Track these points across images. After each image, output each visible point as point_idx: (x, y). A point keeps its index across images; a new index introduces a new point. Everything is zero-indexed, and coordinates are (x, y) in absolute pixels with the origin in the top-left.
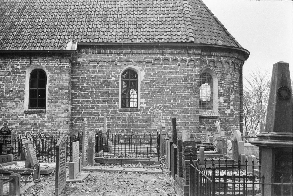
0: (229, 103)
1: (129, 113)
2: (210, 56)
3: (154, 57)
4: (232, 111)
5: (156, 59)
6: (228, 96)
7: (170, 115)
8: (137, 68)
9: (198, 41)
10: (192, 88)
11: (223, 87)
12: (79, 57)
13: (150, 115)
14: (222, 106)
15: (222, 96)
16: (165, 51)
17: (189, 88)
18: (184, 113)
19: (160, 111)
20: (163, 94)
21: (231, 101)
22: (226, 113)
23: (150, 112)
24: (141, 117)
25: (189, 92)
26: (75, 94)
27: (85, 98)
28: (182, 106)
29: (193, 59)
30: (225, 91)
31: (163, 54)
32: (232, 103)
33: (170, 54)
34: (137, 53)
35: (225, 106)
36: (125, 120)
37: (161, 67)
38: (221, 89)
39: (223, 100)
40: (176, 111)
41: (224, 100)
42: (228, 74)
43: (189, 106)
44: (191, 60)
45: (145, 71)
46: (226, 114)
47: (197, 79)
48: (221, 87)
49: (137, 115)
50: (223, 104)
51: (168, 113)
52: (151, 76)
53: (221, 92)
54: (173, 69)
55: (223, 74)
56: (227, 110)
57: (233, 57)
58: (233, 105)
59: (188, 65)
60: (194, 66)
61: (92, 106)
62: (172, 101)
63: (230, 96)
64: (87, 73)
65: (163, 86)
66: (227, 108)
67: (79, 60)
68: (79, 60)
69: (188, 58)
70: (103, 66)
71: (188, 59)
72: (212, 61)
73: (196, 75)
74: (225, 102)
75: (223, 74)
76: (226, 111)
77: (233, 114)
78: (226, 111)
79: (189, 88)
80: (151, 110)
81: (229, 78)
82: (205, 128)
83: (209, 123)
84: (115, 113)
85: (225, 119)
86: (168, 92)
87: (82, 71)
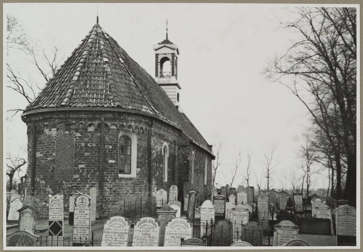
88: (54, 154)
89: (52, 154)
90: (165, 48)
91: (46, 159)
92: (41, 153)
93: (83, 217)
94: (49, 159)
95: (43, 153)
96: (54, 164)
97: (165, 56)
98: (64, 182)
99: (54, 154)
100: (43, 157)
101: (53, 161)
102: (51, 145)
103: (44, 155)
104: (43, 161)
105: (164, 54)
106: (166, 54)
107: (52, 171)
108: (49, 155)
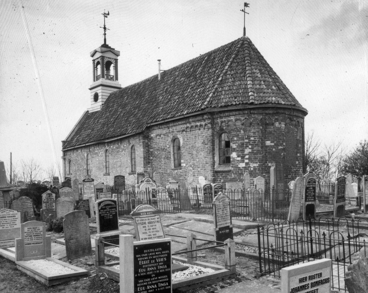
0: (243, 157)
2: (221, 117)
3: (186, 126)
4: (247, 164)
5: (187, 128)
6: (242, 150)
9: (235, 102)
11: (236, 143)
12: (152, 134)
14: (235, 161)
15: (236, 152)
16: (191, 120)
22: (239, 166)
26: (153, 159)
27: (157, 162)
30: (238, 147)
31: (190, 123)
32: (247, 157)
33: (193, 122)
34: (176, 125)
35: (238, 161)
38: (234, 145)
41: (237, 155)
44: (206, 125)
45: (183, 138)
46: (240, 168)
47: (210, 140)
48: (233, 144)
50: (236, 159)
52: (186, 141)
53: (234, 149)
56: (241, 164)
57: (244, 114)
58: (249, 159)
59: (204, 129)
60: (209, 129)
61: (160, 167)
63: (244, 151)
64: (156, 144)
66: (241, 162)
67: (152, 135)
68: (152, 135)
69: (203, 123)
70: (162, 138)
71: (204, 124)
72: (224, 122)
74: (238, 156)
76: (239, 165)
78: (239, 165)
80: (187, 168)
82: (220, 181)
83: (224, 177)
85: (239, 172)
87: (154, 143)
88: (284, 144)
89: (283, 144)
91: (278, 148)
92: (271, 142)
93: (152, 230)
94: (280, 147)
96: (285, 152)
98: (292, 167)
99: (284, 144)
100: (273, 146)
101: (284, 149)
102: (280, 136)
103: (275, 144)
104: (274, 149)
105: (109, 58)
106: (110, 58)
107: (284, 158)
108: (280, 144)
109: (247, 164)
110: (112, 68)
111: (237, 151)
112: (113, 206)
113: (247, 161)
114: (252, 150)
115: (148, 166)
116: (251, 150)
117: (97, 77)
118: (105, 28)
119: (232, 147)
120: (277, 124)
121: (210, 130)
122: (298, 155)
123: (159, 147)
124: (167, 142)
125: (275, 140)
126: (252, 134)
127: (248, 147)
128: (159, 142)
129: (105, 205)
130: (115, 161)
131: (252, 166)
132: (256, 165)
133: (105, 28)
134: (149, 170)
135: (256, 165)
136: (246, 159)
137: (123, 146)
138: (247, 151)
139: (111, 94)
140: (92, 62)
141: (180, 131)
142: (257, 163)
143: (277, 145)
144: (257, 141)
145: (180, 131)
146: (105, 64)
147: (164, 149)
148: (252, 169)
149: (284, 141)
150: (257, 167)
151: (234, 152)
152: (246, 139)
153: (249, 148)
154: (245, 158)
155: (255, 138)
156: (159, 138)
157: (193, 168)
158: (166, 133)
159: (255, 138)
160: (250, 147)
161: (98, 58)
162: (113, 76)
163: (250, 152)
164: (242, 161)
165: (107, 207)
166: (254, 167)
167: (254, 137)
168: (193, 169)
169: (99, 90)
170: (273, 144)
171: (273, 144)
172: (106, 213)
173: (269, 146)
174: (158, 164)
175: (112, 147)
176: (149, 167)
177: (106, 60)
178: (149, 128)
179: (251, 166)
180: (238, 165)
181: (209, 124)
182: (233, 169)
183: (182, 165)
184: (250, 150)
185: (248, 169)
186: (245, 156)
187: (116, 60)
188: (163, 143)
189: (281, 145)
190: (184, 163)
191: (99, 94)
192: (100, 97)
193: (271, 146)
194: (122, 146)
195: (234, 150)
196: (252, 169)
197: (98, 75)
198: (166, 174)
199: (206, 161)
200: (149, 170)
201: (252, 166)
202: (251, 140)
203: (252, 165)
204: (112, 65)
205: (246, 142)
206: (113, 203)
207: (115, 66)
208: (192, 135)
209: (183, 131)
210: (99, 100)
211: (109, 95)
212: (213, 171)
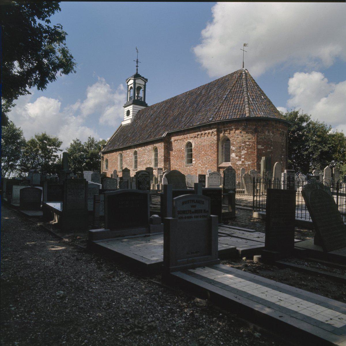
0: (240, 157)
1: (188, 167)
4: (243, 162)
5: (198, 135)
6: (239, 152)
7: (204, 167)
8: (191, 141)
10: (213, 149)
13: (197, 168)
17: (212, 150)
18: (210, 166)
19: (200, 165)
20: (201, 155)
21: (243, 155)
22: (237, 164)
23: (197, 166)
24: (193, 169)
25: (212, 153)
27: (174, 160)
28: (209, 161)
29: (213, 131)
30: (236, 149)
35: (237, 159)
36: (187, 171)
37: (200, 139)
38: (234, 147)
39: (234, 155)
40: (207, 164)
41: (236, 155)
42: (239, 137)
43: (212, 161)
44: (212, 132)
46: (237, 165)
48: (233, 147)
49: (192, 168)
51: (204, 166)
52: (197, 145)
53: (234, 150)
54: (205, 139)
55: (235, 137)
62: (205, 159)
65: (201, 150)
66: (238, 161)
69: (210, 131)
70: (179, 142)
73: (215, 141)
75: (235, 137)
77: (245, 164)
79: (212, 150)
80: (197, 165)
81: (240, 140)
84: (184, 168)
86: (203, 153)
88: (272, 148)
89: (271, 148)
90: (140, 79)
94: (268, 150)
95: (264, 146)
97: (140, 85)
99: (272, 148)
101: (271, 152)
102: (269, 142)
104: (264, 152)
105: (139, 84)
109: (243, 162)
110: (141, 92)
111: (236, 152)
112: (147, 176)
113: (243, 160)
114: (247, 152)
115: (167, 163)
116: (246, 151)
117: (129, 98)
118: (137, 62)
119: (232, 149)
120: (267, 133)
121: (216, 137)
122: (283, 157)
123: (176, 149)
124: (182, 145)
125: (265, 145)
126: (247, 140)
127: (244, 149)
128: (176, 145)
129: (142, 175)
130: (142, 159)
131: (247, 164)
132: (249, 163)
133: (137, 62)
134: (168, 167)
135: (249, 163)
136: (243, 158)
137: (149, 148)
138: (244, 152)
139: (139, 110)
140: (127, 87)
141: (193, 137)
142: (250, 161)
143: (266, 148)
144: (251, 145)
145: (193, 137)
146: (136, 88)
147: (180, 150)
148: (247, 166)
149: (271, 146)
150: (251, 164)
151: (233, 152)
152: (243, 143)
153: (245, 150)
154: (242, 157)
155: (250, 143)
156: (176, 143)
157: (201, 164)
158: (182, 139)
159: (250, 143)
160: (246, 149)
161: (131, 84)
162: (142, 97)
163: (245, 153)
164: (239, 159)
165: (143, 176)
166: (248, 164)
167: (248, 142)
168: (202, 166)
169: (130, 108)
170: (263, 148)
171: (263, 148)
172: (142, 180)
173: (260, 149)
174: (174, 162)
175: (140, 149)
176: (168, 164)
177: (137, 86)
178: (170, 135)
179: (246, 163)
180: (236, 163)
181: (215, 132)
182: (232, 165)
183: (193, 162)
184: (246, 152)
185: (244, 166)
186: (241, 156)
187: (145, 86)
188: (179, 146)
189: (270, 148)
190: (195, 161)
191: (130, 111)
192: (131, 113)
193: (262, 149)
194: (148, 148)
195: (233, 151)
196: (247, 166)
197: (131, 96)
198: (181, 169)
199: (212, 160)
200: (168, 167)
201: (247, 164)
202: (247, 145)
203: (247, 163)
204: (142, 90)
205: (243, 146)
206: (147, 173)
207: (143, 90)
208: (202, 140)
209: (195, 137)
210: (130, 115)
211: (138, 111)
212: (217, 167)
